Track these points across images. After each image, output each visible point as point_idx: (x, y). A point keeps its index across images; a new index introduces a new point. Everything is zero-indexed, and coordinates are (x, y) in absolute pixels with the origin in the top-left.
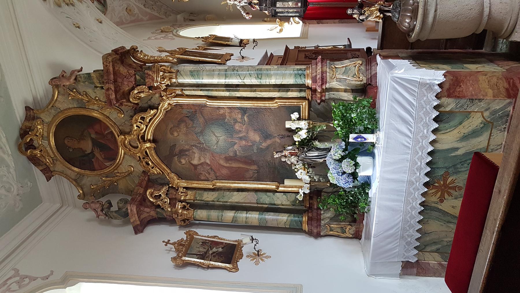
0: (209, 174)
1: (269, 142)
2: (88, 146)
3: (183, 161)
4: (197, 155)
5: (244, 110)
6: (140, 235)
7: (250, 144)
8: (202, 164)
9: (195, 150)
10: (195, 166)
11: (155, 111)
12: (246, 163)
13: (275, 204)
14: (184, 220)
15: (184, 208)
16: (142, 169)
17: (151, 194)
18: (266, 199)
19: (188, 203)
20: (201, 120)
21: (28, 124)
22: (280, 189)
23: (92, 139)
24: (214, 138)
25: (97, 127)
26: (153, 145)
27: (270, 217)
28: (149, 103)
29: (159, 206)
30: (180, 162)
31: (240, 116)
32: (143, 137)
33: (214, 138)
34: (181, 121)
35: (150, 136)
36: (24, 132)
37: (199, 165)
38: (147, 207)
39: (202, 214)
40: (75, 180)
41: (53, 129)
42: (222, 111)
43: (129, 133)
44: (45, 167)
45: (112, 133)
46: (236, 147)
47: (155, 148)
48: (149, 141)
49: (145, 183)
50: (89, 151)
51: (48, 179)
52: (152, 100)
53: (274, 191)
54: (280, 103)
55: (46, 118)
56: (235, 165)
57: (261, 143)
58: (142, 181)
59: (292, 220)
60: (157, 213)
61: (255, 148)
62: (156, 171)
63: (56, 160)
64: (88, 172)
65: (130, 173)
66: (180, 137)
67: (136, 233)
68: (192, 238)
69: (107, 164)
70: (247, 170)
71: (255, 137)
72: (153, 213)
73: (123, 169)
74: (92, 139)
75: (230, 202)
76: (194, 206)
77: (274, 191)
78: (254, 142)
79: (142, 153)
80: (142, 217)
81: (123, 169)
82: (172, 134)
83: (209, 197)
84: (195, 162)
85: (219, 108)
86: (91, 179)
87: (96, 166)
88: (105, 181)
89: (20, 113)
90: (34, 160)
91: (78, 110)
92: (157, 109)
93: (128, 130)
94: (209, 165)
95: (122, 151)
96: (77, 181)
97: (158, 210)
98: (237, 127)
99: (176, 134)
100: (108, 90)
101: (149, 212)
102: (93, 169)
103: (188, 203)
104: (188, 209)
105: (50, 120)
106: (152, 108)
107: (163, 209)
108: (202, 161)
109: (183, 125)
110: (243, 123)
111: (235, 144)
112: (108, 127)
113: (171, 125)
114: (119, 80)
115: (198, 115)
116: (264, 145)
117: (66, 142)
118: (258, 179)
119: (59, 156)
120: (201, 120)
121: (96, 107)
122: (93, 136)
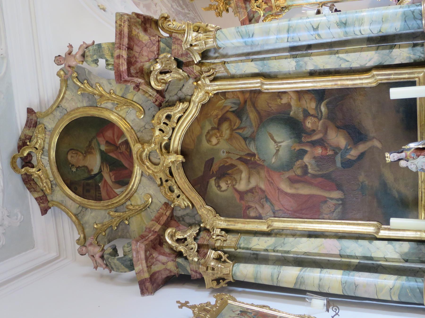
0: (263, 206)
1: (362, 147)
2: (94, 163)
3: (223, 186)
4: (244, 175)
5: (320, 95)
6: (148, 298)
7: (330, 153)
8: (251, 191)
9: (242, 167)
10: (242, 194)
11: (186, 104)
12: (322, 187)
13: (371, 258)
14: (218, 280)
15: (219, 259)
16: (163, 200)
17: (172, 236)
18: (357, 249)
19: (225, 253)
20: (252, 115)
21: (28, 133)
22: (383, 233)
23: (102, 152)
24: (272, 146)
25: (109, 134)
26: (181, 158)
27: (363, 279)
28: (180, 94)
29: (180, 254)
30: (219, 187)
31: (313, 105)
32: (167, 147)
33: (272, 146)
34: (223, 120)
35: (176, 143)
36: (23, 143)
37: (247, 192)
38: (164, 254)
39: (245, 271)
40: (76, 215)
41: (56, 139)
42: (284, 101)
43: (149, 142)
44: (41, 194)
45: (126, 143)
46: (307, 159)
47: (182, 163)
48: (176, 153)
49: (164, 218)
50: (96, 171)
51: (44, 211)
52: (184, 90)
53: (372, 238)
54: (382, 76)
55: (49, 123)
56: (305, 190)
57: (347, 150)
58: (162, 215)
59: (402, 288)
60: (178, 266)
61: (338, 159)
62: (183, 202)
63: (56, 185)
64: (92, 203)
65: (146, 207)
66: (220, 146)
67: (143, 293)
68: (224, 304)
69: (117, 191)
70: (325, 200)
71: (339, 139)
72: (171, 266)
73: (138, 200)
74: (102, 152)
75: (295, 253)
76: (235, 258)
77: (372, 238)
78: (336, 150)
79: (164, 172)
80: (155, 268)
81: (138, 200)
82: (209, 141)
83: (259, 244)
84: (242, 186)
85: (280, 94)
86: (97, 215)
87: (104, 194)
88: (113, 217)
89: (21, 118)
90: (29, 181)
91: (87, 109)
92: (190, 102)
93: (147, 138)
94: (263, 191)
95: (137, 170)
96: (78, 219)
97: (180, 260)
98: (309, 124)
99: (214, 141)
100: (119, 57)
101: (165, 264)
102: (99, 199)
103: (225, 253)
104: (225, 262)
105: (53, 126)
106: (181, 100)
107: (186, 258)
108: (253, 183)
109: (225, 126)
110: (318, 116)
111: (305, 152)
112: (121, 134)
113: (208, 127)
114: (136, 49)
115: (249, 108)
116: (354, 153)
117: (69, 157)
118: (344, 216)
119: (60, 180)
120: (252, 115)
121: (109, 105)
122: (103, 148)
